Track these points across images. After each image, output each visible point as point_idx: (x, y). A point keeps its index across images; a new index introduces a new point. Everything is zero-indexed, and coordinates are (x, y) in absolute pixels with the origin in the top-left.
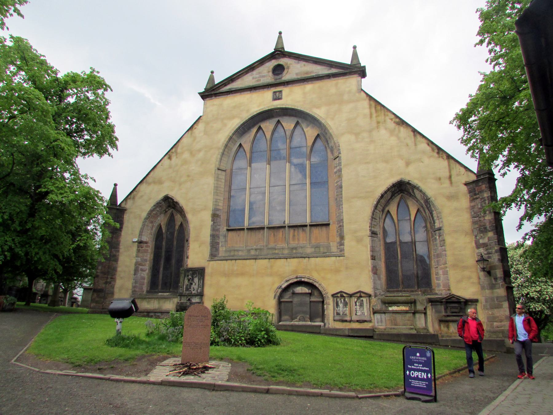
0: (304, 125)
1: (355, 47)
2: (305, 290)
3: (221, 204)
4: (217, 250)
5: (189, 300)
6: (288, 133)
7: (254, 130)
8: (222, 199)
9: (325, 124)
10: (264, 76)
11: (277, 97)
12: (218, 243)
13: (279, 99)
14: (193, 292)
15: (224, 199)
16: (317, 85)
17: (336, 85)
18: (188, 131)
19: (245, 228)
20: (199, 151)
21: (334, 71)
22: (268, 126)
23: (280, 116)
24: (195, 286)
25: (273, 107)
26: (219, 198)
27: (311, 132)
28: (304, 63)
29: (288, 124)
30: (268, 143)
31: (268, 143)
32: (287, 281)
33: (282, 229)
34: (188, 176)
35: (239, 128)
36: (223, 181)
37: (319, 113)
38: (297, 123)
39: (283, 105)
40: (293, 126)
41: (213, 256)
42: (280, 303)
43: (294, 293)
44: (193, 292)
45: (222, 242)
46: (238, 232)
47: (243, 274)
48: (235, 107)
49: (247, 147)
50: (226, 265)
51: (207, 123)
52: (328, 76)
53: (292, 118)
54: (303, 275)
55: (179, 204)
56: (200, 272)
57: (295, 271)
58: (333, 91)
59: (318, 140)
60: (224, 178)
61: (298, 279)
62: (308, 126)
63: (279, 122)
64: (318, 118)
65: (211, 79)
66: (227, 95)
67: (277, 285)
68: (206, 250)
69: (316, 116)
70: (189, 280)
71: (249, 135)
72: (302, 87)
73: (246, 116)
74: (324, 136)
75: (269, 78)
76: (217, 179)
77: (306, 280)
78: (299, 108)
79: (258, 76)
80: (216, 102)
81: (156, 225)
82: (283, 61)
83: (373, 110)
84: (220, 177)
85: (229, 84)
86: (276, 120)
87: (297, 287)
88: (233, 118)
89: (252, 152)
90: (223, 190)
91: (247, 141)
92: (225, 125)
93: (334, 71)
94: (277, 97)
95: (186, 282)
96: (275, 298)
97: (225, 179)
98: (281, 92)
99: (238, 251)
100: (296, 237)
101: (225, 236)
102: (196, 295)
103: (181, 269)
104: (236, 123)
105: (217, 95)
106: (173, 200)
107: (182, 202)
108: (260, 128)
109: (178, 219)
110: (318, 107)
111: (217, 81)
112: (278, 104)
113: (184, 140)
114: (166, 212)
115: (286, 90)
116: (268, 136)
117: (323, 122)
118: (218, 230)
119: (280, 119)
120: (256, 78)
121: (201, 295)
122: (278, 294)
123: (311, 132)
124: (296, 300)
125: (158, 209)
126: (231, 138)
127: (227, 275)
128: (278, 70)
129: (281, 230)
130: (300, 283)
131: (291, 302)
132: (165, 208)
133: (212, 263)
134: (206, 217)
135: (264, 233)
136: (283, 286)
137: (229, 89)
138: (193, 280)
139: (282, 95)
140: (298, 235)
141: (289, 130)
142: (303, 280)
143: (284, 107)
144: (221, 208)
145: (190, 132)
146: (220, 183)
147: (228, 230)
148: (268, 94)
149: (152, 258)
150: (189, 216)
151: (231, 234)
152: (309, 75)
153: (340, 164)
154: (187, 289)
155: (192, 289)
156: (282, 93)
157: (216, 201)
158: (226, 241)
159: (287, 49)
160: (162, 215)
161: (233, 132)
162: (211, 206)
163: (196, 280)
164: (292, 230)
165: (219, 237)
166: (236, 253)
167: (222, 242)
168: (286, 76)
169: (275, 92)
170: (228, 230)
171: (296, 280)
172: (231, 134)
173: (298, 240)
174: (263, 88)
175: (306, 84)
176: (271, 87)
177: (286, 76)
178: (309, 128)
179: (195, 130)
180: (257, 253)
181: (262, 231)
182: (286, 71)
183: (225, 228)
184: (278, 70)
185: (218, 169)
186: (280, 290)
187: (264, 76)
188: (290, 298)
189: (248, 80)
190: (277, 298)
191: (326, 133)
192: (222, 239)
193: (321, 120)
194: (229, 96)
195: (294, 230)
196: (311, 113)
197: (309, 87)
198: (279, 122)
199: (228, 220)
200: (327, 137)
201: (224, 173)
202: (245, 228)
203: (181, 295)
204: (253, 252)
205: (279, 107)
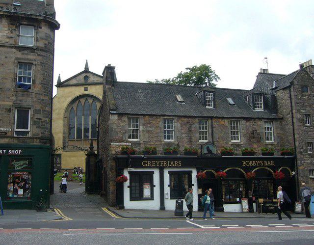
7: (78, 101)
11: (86, 90)
13: (87, 90)
20: (57, 109)
22: (83, 101)
24: (58, 160)
29: (90, 101)
49: (75, 108)
51: (59, 98)
56: (59, 156)
63: (87, 99)
71: (75, 104)
73: (74, 96)
75: (83, 81)
76: (64, 121)
80: (62, 89)
82: (87, 74)
89: (77, 111)
91: (75, 106)
94: (86, 90)
104: (70, 99)
105: (62, 86)
108: (79, 101)
111: (62, 81)
112: (86, 92)
115: (89, 87)
121: (60, 163)
126: (69, 105)
127: (70, 157)
128: (86, 78)
148: (82, 88)
157: (64, 130)
159: (90, 70)
162: (62, 131)
163: (58, 159)
169: (85, 88)
184: (86, 78)
189: (74, 82)
198: (87, 99)
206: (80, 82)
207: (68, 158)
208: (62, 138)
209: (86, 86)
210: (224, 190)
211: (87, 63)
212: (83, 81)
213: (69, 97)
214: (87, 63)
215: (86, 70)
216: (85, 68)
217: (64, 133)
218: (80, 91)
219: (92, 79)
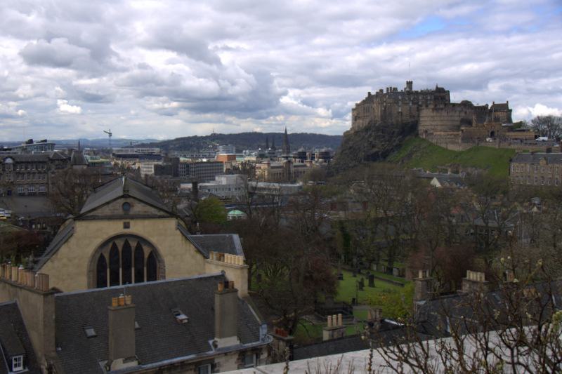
10: (117, 210)
11: (127, 226)
37: (153, 240)
52: (160, 217)
62: (145, 245)
73: (106, 237)
76: (89, 278)
82: (129, 200)
83: (184, 242)
93: (162, 213)
94: (127, 226)
98: (129, 223)
104: (99, 241)
112: (127, 231)
115: (132, 223)
126: (96, 251)
128: (127, 206)
153: (164, 273)
169: (125, 223)
184: (127, 206)
187: (117, 210)
189: (107, 211)
197: (147, 222)
209: (127, 221)
210: (258, 319)
212: (120, 212)
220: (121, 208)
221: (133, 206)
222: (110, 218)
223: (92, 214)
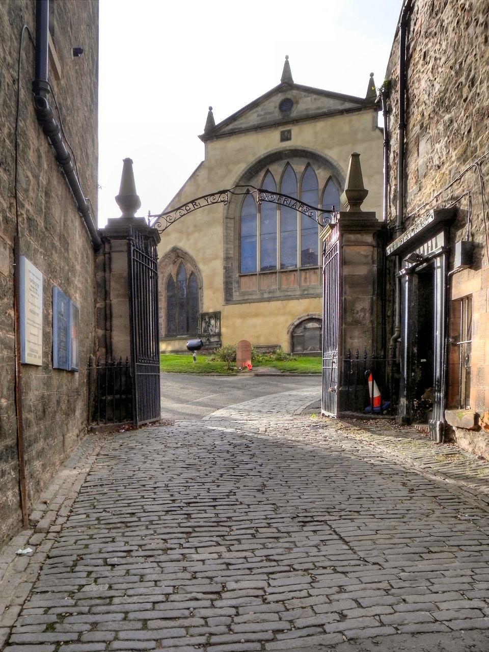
0: (315, 167)
1: (372, 75)
2: (316, 325)
3: (231, 252)
4: (231, 295)
5: (208, 340)
6: (298, 176)
7: (262, 174)
8: (232, 247)
9: (337, 166)
11: (286, 137)
12: (231, 289)
13: (289, 139)
14: (211, 333)
15: (234, 247)
16: (330, 121)
17: (350, 121)
18: (190, 178)
19: (258, 273)
21: (348, 105)
22: (277, 169)
23: (289, 157)
25: (282, 149)
26: (229, 246)
27: (322, 175)
28: (315, 96)
29: (299, 167)
30: (278, 187)
31: (278, 187)
32: (299, 319)
33: (295, 273)
34: (195, 226)
35: (246, 173)
36: (232, 229)
38: (308, 165)
39: (291, 146)
40: (303, 168)
41: (228, 299)
42: (292, 337)
43: (305, 328)
44: (211, 333)
45: (235, 288)
46: (251, 277)
47: (257, 315)
48: (239, 150)
50: (243, 308)
51: (210, 169)
52: (342, 112)
53: (303, 159)
54: (314, 313)
55: (188, 255)
56: (217, 316)
57: (306, 310)
58: (346, 128)
59: (330, 181)
60: (233, 225)
61: (310, 317)
62: (319, 167)
64: (330, 160)
65: (210, 118)
66: (230, 136)
67: (289, 323)
68: (221, 296)
69: (328, 158)
70: (206, 323)
72: (313, 124)
73: (252, 159)
74: (337, 179)
75: (277, 115)
76: (226, 228)
77: (317, 317)
78: (310, 150)
79: (262, 113)
80: (218, 144)
81: (166, 275)
84: (229, 225)
85: (231, 123)
86: (285, 161)
87: (308, 323)
88: (238, 162)
90: (232, 238)
92: (230, 171)
94: (286, 137)
95: (204, 325)
96: (288, 333)
97: (234, 227)
98: (289, 131)
99: (251, 294)
100: (308, 280)
101: (238, 282)
102: (214, 336)
103: (198, 314)
106: (182, 251)
107: (192, 253)
108: (268, 171)
109: (189, 267)
110: (330, 148)
111: (217, 121)
112: (287, 145)
113: (187, 188)
114: (175, 262)
115: (295, 130)
116: (277, 179)
117: (335, 164)
118: (230, 277)
119: (289, 160)
120: (261, 115)
122: (291, 330)
123: (322, 175)
124: (307, 334)
125: (167, 260)
127: (243, 316)
128: (286, 105)
129: (292, 274)
130: (311, 320)
131: (303, 336)
132: (174, 258)
133: (227, 307)
134: (218, 265)
135: (276, 277)
136: (296, 324)
137: (232, 129)
138: (210, 323)
139: (291, 135)
140: (310, 277)
141: (300, 172)
142: (314, 317)
143: (293, 148)
144: (232, 256)
145: (193, 180)
146: (229, 232)
147: (240, 276)
149: (166, 306)
150: (201, 266)
151: (243, 279)
152: (320, 111)
154: (205, 331)
155: (210, 331)
156: (291, 132)
157: (227, 251)
158: (239, 287)
159: (297, 80)
160: (171, 265)
161: (239, 178)
162: (221, 254)
164: (303, 274)
165: (232, 283)
166: (250, 297)
167: (235, 288)
168: (295, 113)
169: (283, 133)
170: (240, 276)
171: (307, 318)
172: (237, 181)
173: (310, 282)
174: (270, 128)
175: (316, 122)
176: (278, 126)
177: (295, 113)
178: (320, 170)
179: (197, 178)
180: (270, 296)
181: (274, 276)
182: (295, 106)
183: (237, 275)
185: (227, 218)
186: (293, 327)
188: (302, 332)
189: (253, 119)
190: (290, 333)
191: (339, 176)
192: (235, 285)
193: (333, 162)
194: (232, 137)
195: (306, 273)
196: (322, 154)
197: (320, 125)
198: (288, 163)
199: (240, 267)
200: (340, 179)
201: (232, 221)
202: (258, 273)
203: (200, 336)
204: (266, 296)
205: (288, 148)
206: (269, 118)
207: (238, 322)
208: (221, 272)
209: (287, 128)
211: (287, 65)
212: (277, 115)
213: (238, 162)
214: (287, 65)
215: (287, 83)
216: (283, 79)
217: (227, 259)
218: (270, 142)
219: (305, 105)
220: (277, 109)
221: (297, 103)
222: (258, 128)
223: (230, 127)
